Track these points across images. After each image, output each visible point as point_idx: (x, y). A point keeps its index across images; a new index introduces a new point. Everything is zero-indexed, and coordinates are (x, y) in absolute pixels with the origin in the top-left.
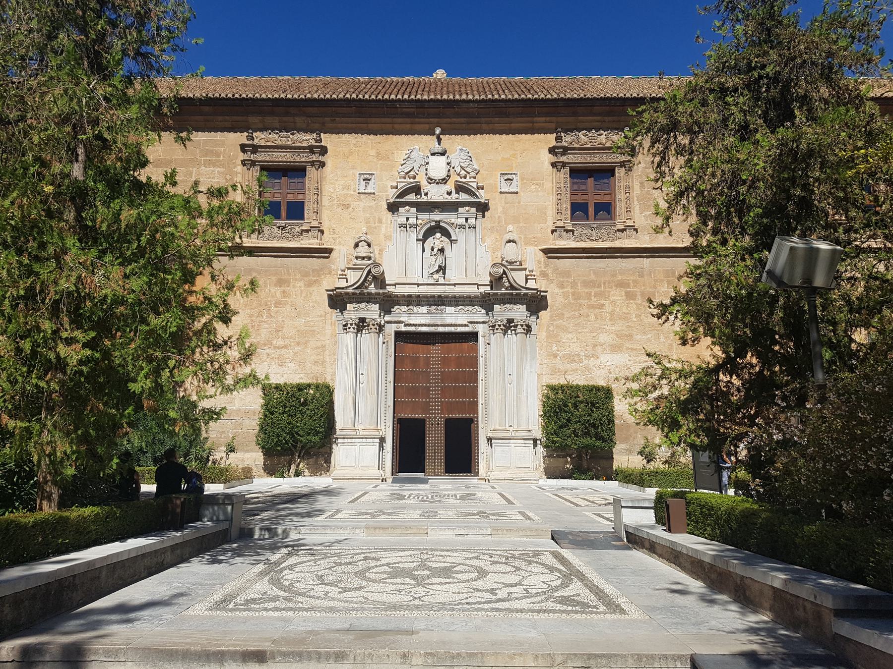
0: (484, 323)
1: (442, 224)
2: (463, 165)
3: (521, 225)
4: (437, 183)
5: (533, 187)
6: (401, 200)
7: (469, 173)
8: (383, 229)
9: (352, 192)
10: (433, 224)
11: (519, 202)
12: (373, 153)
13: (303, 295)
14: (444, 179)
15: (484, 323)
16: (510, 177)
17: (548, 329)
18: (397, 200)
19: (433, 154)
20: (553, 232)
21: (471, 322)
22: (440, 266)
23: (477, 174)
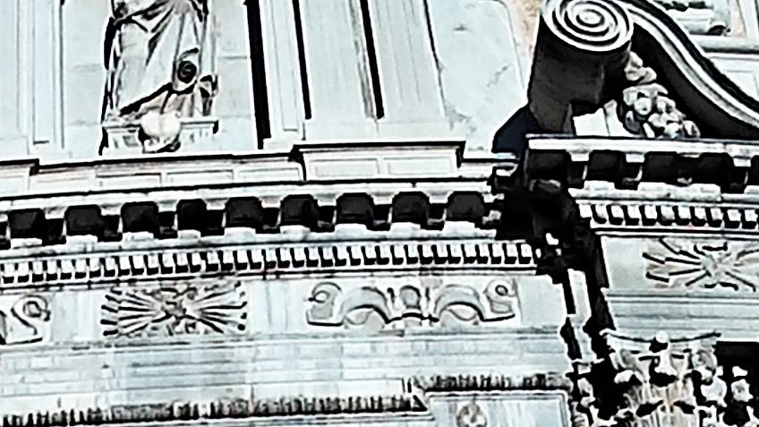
0: (538, 384)
21: (448, 386)
22: (185, 71)
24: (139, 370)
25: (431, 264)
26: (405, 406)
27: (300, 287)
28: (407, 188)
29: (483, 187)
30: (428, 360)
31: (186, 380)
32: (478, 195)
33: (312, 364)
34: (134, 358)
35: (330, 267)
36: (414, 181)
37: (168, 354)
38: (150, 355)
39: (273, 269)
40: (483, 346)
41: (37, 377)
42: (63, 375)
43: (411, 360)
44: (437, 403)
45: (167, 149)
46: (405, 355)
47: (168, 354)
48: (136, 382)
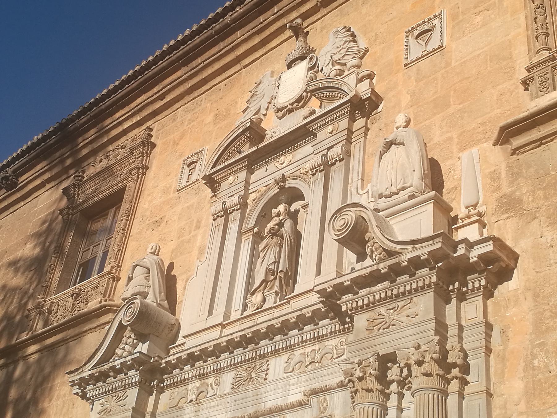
1: (290, 184)
2: (335, 57)
3: (451, 110)
4: (290, 111)
5: (479, 19)
6: (220, 167)
7: (345, 64)
8: (199, 238)
9: (171, 195)
10: (276, 190)
11: (448, 64)
12: (210, 118)
13: (64, 410)
14: (298, 100)
15: (341, 385)
16: (426, 27)
17: (529, 367)
18: (212, 171)
19: (289, 66)
20: (526, 83)
21: (315, 392)
23: (361, 58)
24: (237, 402)
25: (320, 339)
26: (301, 404)
27: (285, 357)
28: (299, 313)
29: (321, 305)
30: (314, 381)
31: (248, 404)
32: (319, 309)
33: (280, 391)
34: (234, 398)
35: (291, 348)
36: (301, 310)
37: (243, 395)
38: (239, 397)
39: (276, 353)
40: (330, 371)
41: (212, 410)
42: (219, 408)
43: (308, 383)
44: (314, 400)
45: (258, 309)
46: (307, 381)
47: (243, 395)
48: (236, 407)
